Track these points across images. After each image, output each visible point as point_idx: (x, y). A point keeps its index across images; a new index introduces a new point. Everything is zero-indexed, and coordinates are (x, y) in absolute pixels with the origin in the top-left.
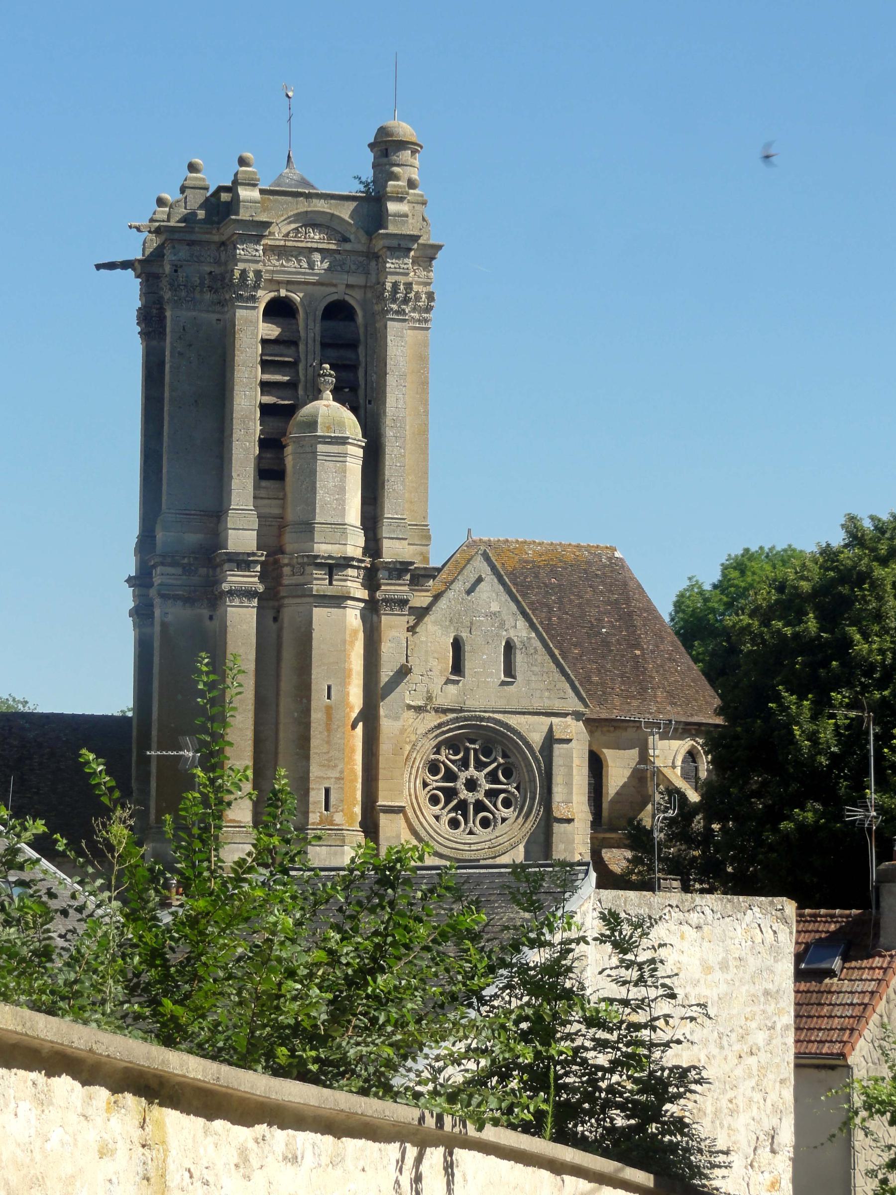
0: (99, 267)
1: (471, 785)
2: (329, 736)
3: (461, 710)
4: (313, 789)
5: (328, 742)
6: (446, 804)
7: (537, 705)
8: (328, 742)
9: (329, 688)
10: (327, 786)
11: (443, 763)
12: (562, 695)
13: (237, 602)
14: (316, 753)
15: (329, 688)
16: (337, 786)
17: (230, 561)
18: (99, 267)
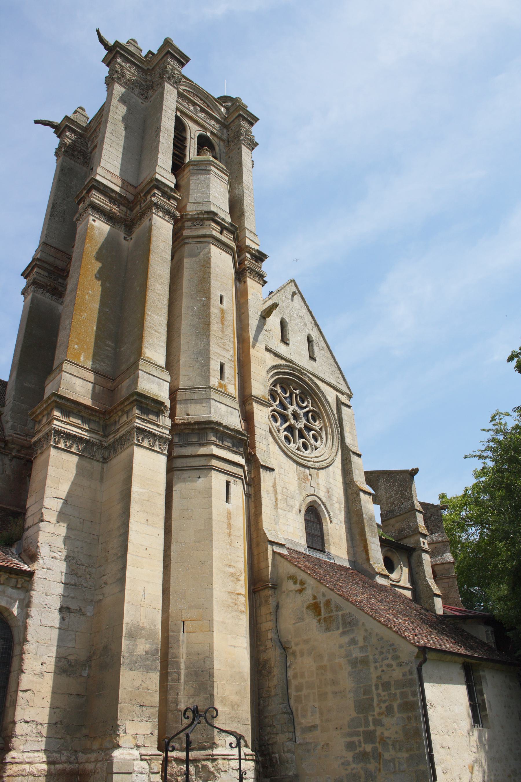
0: (37, 122)
1: (296, 416)
2: (223, 328)
3: (291, 362)
4: (213, 359)
5: (223, 331)
6: (281, 425)
7: (328, 379)
8: (223, 331)
9: (222, 298)
10: (223, 361)
11: (278, 394)
12: (338, 381)
13: (161, 214)
14: (215, 335)
15: (222, 298)
16: (229, 365)
17: (158, 188)
18: (37, 122)
